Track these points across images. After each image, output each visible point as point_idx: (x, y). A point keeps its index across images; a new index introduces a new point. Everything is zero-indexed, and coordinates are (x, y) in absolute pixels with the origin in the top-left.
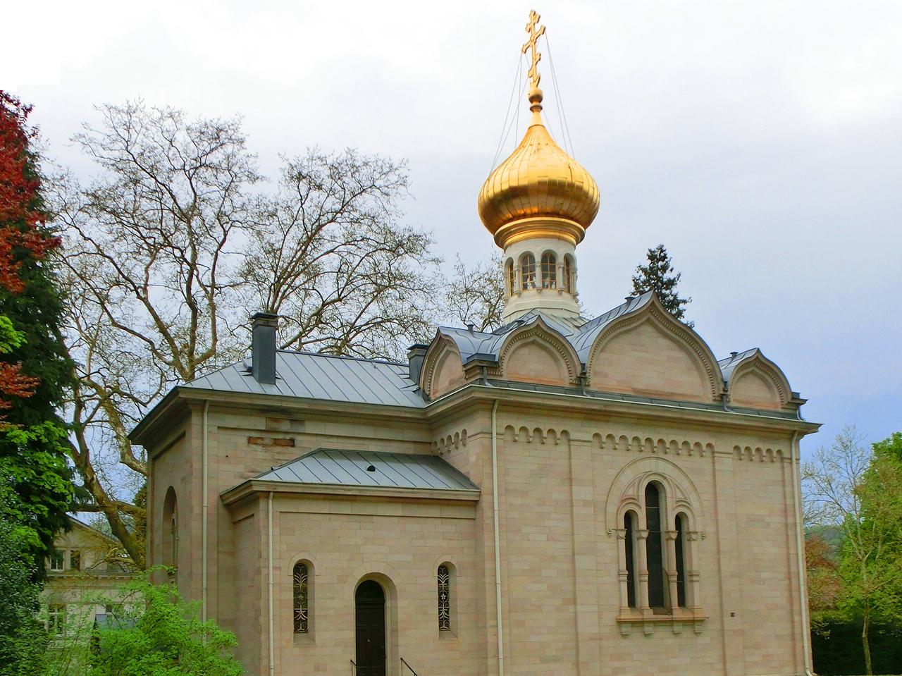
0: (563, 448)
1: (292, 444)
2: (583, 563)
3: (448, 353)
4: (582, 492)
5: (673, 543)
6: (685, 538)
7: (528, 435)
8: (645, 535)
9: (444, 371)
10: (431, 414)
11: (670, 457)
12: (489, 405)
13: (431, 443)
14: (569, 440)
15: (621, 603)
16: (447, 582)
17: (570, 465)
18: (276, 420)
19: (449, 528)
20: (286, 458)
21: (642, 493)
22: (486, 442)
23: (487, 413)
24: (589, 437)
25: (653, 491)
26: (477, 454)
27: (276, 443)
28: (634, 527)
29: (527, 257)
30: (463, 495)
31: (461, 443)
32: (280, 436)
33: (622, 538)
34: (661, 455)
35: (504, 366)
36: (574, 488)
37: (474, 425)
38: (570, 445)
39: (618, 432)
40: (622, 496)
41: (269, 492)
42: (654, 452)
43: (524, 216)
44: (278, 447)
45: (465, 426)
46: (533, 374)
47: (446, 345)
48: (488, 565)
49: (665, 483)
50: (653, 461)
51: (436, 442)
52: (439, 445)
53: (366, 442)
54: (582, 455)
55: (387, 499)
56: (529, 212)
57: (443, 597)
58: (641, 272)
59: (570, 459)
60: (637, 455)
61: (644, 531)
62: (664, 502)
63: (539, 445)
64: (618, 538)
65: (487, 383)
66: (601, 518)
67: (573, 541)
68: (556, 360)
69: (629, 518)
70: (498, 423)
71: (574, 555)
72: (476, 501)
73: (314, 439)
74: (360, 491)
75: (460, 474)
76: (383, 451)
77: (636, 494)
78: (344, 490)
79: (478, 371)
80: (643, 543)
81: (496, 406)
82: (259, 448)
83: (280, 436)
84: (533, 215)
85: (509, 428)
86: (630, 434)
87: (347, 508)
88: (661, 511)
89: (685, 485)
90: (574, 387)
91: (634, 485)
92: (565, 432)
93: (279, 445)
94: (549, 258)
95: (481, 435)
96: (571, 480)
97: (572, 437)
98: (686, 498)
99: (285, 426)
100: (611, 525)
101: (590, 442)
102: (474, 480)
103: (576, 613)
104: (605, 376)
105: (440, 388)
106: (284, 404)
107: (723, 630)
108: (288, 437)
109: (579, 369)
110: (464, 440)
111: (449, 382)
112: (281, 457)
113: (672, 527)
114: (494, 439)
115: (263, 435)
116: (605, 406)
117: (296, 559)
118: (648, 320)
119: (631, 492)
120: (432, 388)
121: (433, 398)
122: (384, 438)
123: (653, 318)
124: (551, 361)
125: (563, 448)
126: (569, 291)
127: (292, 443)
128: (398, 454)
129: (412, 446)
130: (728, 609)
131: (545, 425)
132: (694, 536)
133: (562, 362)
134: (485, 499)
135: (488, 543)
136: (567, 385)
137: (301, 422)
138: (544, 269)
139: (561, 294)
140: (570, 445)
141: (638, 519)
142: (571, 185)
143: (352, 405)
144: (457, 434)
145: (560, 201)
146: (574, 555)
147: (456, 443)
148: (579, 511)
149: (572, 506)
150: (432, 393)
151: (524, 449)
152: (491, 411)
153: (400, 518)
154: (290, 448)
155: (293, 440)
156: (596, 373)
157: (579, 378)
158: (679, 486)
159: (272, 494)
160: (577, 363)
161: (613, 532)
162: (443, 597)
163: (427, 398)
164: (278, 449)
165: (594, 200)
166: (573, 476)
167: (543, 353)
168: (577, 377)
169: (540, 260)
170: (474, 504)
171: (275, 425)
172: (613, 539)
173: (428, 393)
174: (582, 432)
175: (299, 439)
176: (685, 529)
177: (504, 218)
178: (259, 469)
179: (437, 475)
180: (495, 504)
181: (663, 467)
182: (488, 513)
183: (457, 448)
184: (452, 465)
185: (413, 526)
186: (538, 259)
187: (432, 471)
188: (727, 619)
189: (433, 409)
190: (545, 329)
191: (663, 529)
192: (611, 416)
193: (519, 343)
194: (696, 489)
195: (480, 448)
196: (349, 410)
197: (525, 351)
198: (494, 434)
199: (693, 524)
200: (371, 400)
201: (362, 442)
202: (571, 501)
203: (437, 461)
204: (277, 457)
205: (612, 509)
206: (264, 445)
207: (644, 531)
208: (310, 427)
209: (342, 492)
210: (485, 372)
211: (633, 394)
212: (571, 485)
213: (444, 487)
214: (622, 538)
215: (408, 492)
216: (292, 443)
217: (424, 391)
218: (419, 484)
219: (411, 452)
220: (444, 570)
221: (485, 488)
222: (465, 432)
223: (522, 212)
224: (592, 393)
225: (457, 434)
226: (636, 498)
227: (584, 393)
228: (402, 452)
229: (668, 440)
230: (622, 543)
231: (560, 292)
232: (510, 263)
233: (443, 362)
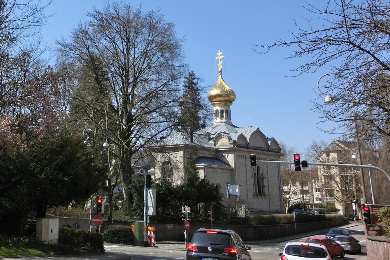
2: (248, 183)
8: (257, 177)
69: (255, 173)
71: (247, 181)
100: (252, 175)
103: (247, 193)
107: (269, 198)
113: (261, 176)
125: (244, 159)
130: (270, 194)
135: (235, 178)
146: (247, 181)
148: (247, 172)
166: (247, 165)
188: (270, 196)
199: (265, 175)
202: (246, 170)
205: (252, 172)
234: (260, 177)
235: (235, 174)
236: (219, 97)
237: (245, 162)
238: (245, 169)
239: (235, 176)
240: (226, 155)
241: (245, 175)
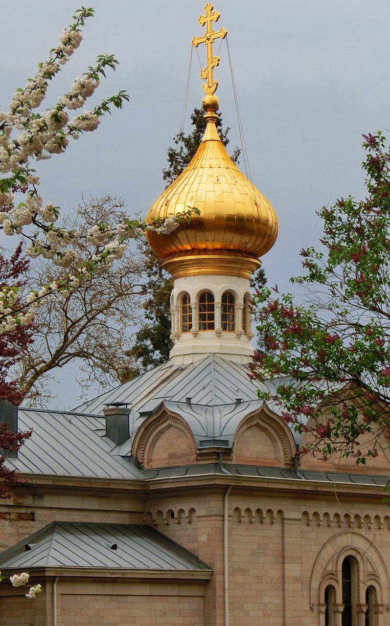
0: (277, 527)
1: (32, 518)
3: (170, 426)
4: (293, 570)
5: (363, 616)
6: (373, 610)
7: (250, 516)
8: (341, 609)
9: (160, 443)
10: (153, 487)
11: (363, 532)
12: (222, 490)
13: (143, 513)
14: (283, 519)
17: (283, 544)
18: (22, 495)
19: (185, 605)
20: (27, 532)
21: (340, 568)
22: (219, 524)
23: (221, 498)
24: (299, 515)
25: (349, 564)
26: (208, 535)
27: (20, 517)
28: (332, 601)
29: (206, 297)
30: (200, 575)
31: (187, 520)
32: (23, 511)
33: (322, 612)
34: (356, 530)
35: (234, 451)
36: (286, 565)
37: (205, 507)
38: (283, 524)
39: (322, 508)
40: (324, 573)
41: (55, 577)
42: (350, 527)
43: (205, 251)
44: (22, 521)
45: (194, 505)
46: (254, 455)
47: (168, 419)
49: (359, 558)
50: (349, 536)
51: (149, 513)
52: (155, 517)
53: (91, 514)
54: (293, 531)
55: (139, 580)
56: (210, 246)
58: (182, 144)
59: (283, 537)
60: (337, 531)
61: (340, 605)
62: (356, 573)
63: (258, 525)
64: (319, 612)
65: (223, 470)
66: (306, 593)
67: (284, 617)
68: (273, 440)
69: (329, 590)
70: (230, 504)
72: (210, 580)
73: (49, 512)
74: (123, 573)
75: (183, 549)
76: (104, 522)
77: (335, 569)
78: (112, 573)
79: (214, 457)
80: (340, 616)
81: (229, 491)
82: (7, 523)
83: (23, 511)
84: (215, 251)
85: (237, 509)
86: (332, 512)
87: (108, 589)
88: (352, 584)
89: (375, 558)
90: (288, 467)
91: (333, 561)
92: (280, 512)
93: (23, 519)
94: (229, 298)
95: (214, 518)
96: (283, 557)
97: (286, 517)
98: (375, 572)
99: (28, 501)
100: (314, 601)
101: (299, 520)
102: (207, 561)
105: (154, 457)
106: (34, 482)
108: (29, 511)
110: (190, 517)
111: (168, 454)
112: (25, 531)
113: (363, 600)
114: (226, 522)
115: (11, 510)
116: (316, 487)
119: (330, 568)
120: (146, 457)
121: (146, 467)
122: (106, 509)
124: (269, 442)
125: (277, 527)
126: (245, 334)
127: (32, 517)
128: (117, 525)
129: (127, 516)
131: (265, 505)
132: (381, 609)
133: (279, 443)
134: (218, 578)
136: (282, 466)
137: (40, 496)
138: (224, 309)
139: (239, 338)
140: (283, 524)
141: (335, 594)
142: (258, 221)
143: (87, 480)
144: (181, 511)
145: (246, 239)
147: (179, 518)
148: (289, 587)
149: (284, 582)
150: (146, 461)
151: (247, 529)
152: (224, 495)
153: (148, 597)
154: (31, 522)
155: (33, 514)
157: (293, 459)
158: (371, 561)
159: (58, 579)
160: (292, 445)
161: (316, 607)
163: (139, 466)
164: (22, 523)
165: (274, 228)
166: (287, 554)
167: (263, 434)
168: (292, 458)
169: (220, 301)
170: (205, 583)
171: (20, 501)
172: (316, 613)
173: (141, 461)
174: (293, 511)
175: (38, 512)
176: (373, 602)
177: (180, 247)
178: (7, 544)
179: (151, 542)
180: (228, 584)
181: (360, 544)
182: (219, 592)
183: (178, 523)
184: (172, 539)
185: (159, 605)
186: (218, 299)
187: (147, 540)
189: (163, 483)
190: (268, 413)
191: (354, 601)
192: (317, 494)
193: (245, 427)
194: (384, 562)
195: (202, 527)
196: (84, 485)
197: (249, 433)
198: (226, 518)
200: (101, 474)
201: (86, 513)
202: (283, 577)
203: (148, 531)
204: (20, 532)
205: (315, 584)
206: (11, 520)
207: (340, 605)
208: (48, 501)
209: (109, 575)
210: (221, 458)
211: (334, 471)
212: (283, 563)
213: (185, 569)
214: (322, 612)
215: (157, 574)
216: (32, 517)
217: (136, 458)
218: (166, 567)
219: (127, 522)
221: (218, 566)
222: (192, 510)
223: (203, 246)
224: (303, 473)
225: (181, 511)
226: (334, 573)
227: (298, 474)
228: (119, 522)
229: (362, 515)
230: (323, 617)
231: (239, 336)
232: (189, 303)
233: (161, 433)
234: (359, 605)
235: (219, 599)
236: (191, 233)
237: (278, 540)
238: (274, 572)
239: (219, 612)
240: (186, 506)
241: (279, 601)
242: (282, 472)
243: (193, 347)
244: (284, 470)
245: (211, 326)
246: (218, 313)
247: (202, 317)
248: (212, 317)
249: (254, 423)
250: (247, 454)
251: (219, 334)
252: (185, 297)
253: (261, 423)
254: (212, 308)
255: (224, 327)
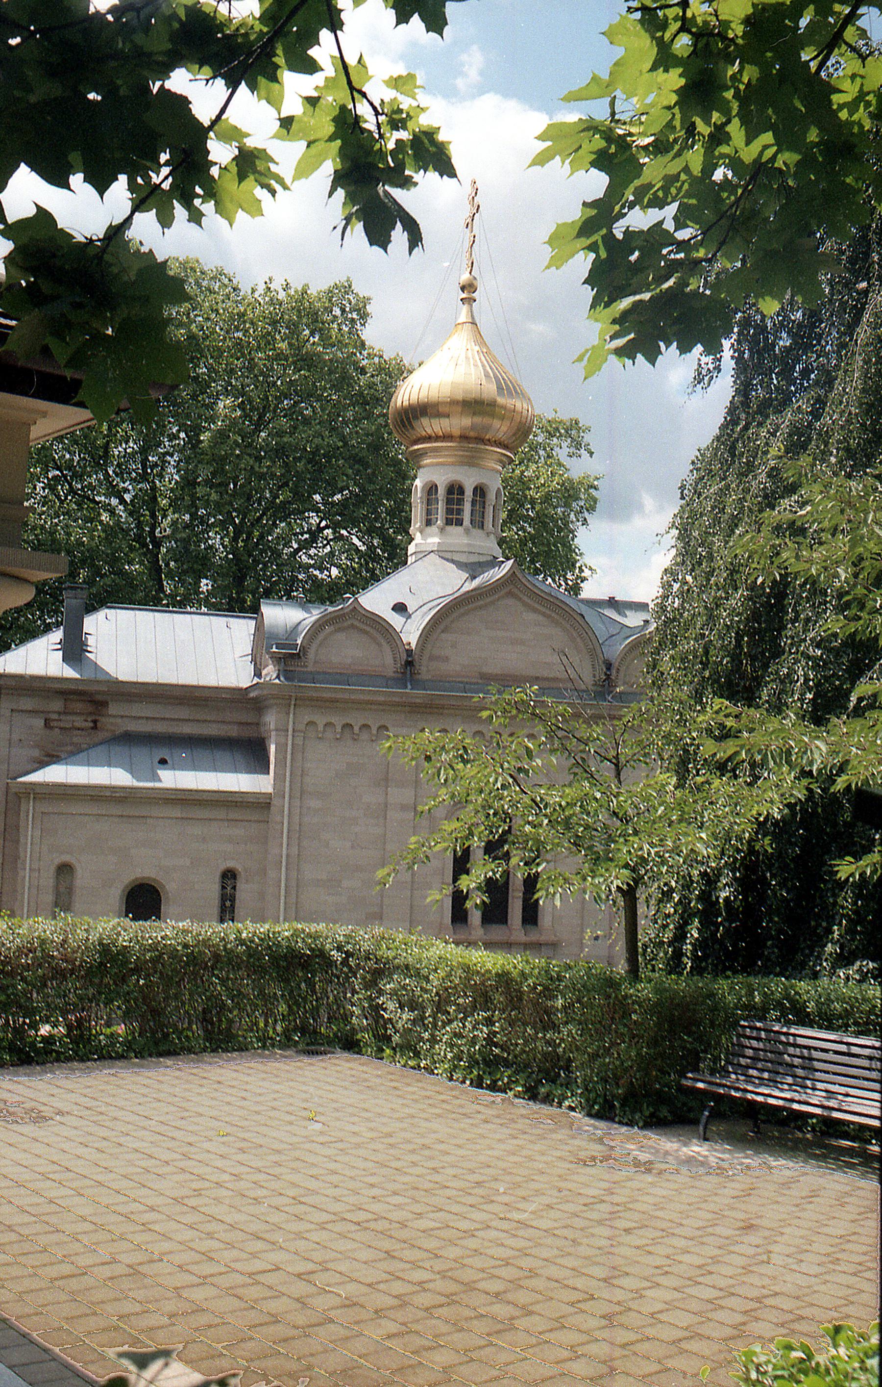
15: (442, 918)
16: (234, 888)
19: (238, 831)
46: (349, 661)
48: (271, 874)
57: (228, 903)
68: (379, 645)
85: (311, 723)
87: (116, 810)
104: (446, 659)
109: (404, 656)
117: (57, 862)
118: (510, 594)
123: (516, 591)
131: (356, 719)
136: (390, 673)
138: (449, 501)
156: (432, 658)
162: (228, 903)
197: (341, 636)
220: (229, 876)
242: (387, 681)
243: (469, 545)
244: (394, 679)
245: (460, 523)
246: (467, 507)
247: (449, 511)
248: (460, 512)
249: (349, 622)
250: (335, 660)
251: (467, 531)
252: (431, 489)
253: (356, 623)
254: (460, 502)
255: (449, 522)
